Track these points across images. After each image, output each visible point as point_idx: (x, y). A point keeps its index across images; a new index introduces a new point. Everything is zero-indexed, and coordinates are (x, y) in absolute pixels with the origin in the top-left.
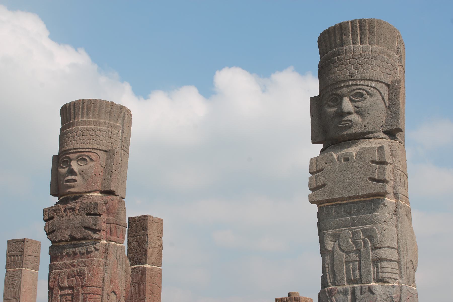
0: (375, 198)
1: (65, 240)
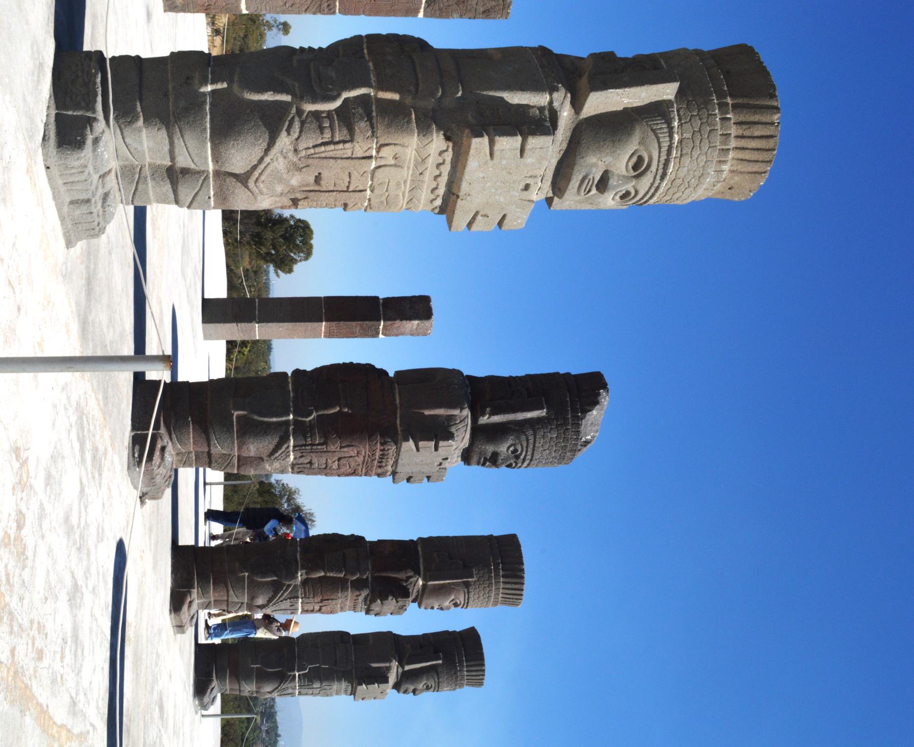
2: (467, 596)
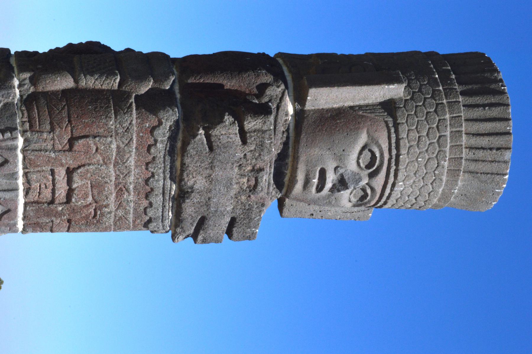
1: (184, 179)
2: (393, 136)
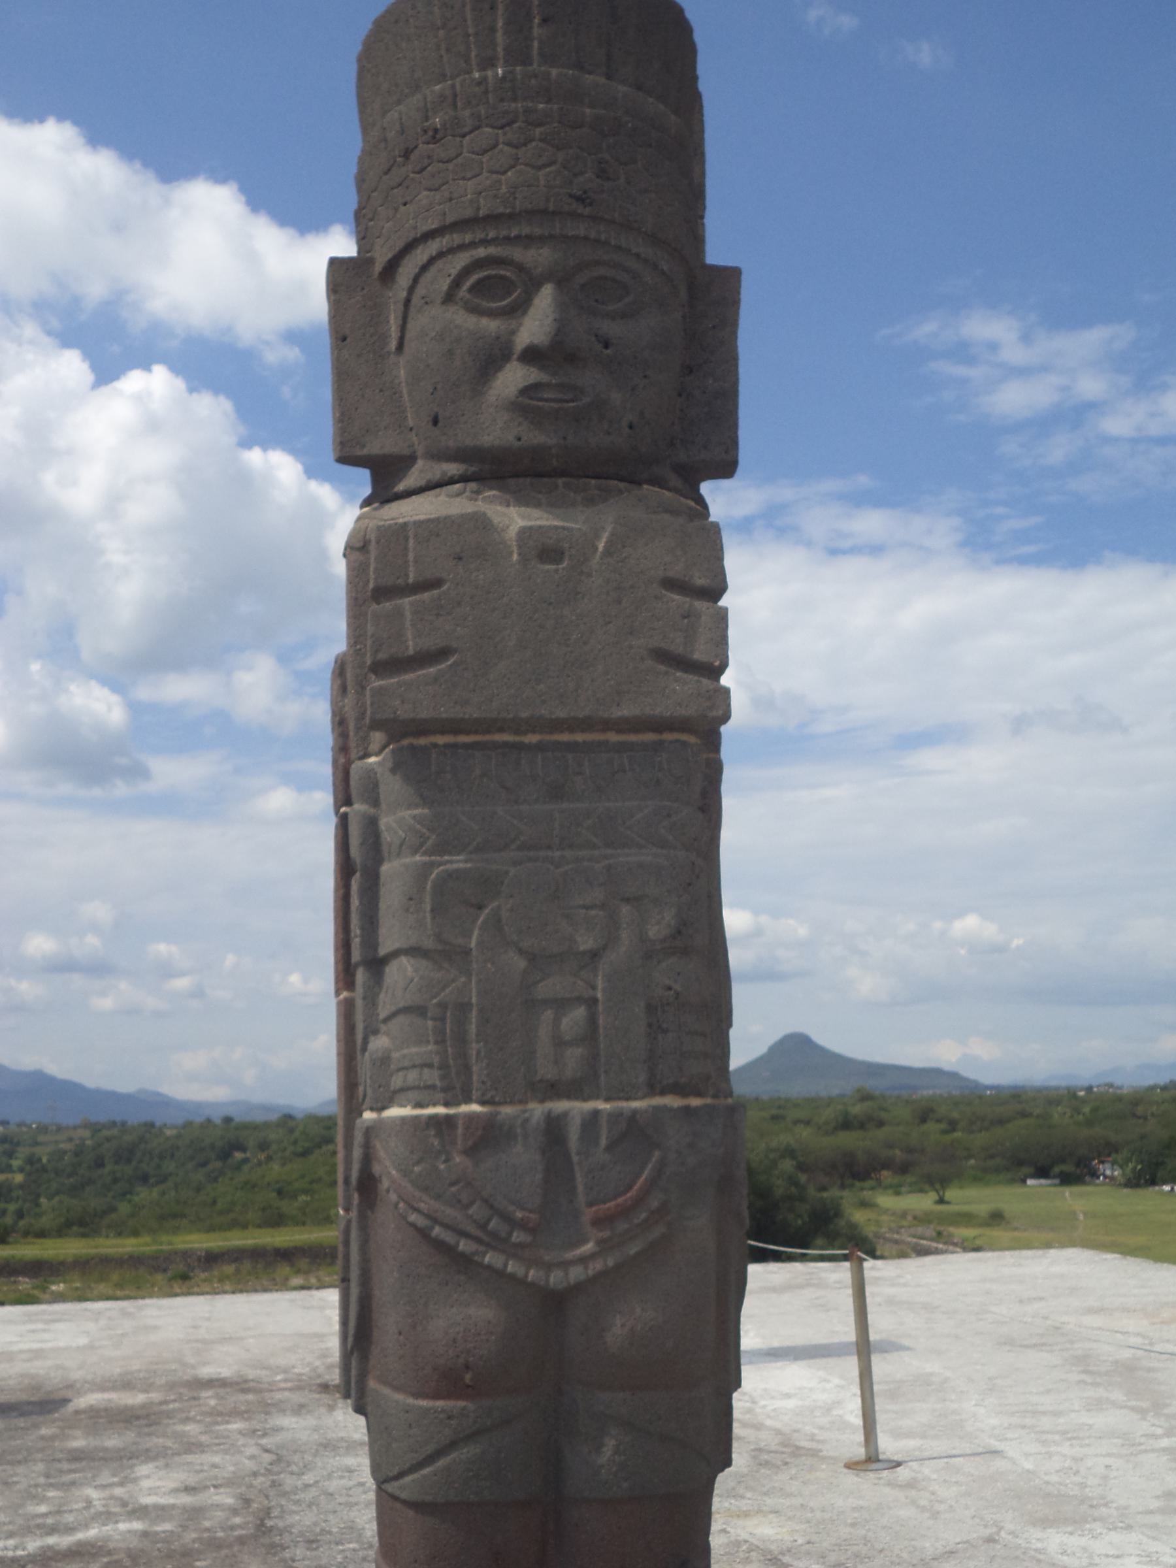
0: (668, 736)
